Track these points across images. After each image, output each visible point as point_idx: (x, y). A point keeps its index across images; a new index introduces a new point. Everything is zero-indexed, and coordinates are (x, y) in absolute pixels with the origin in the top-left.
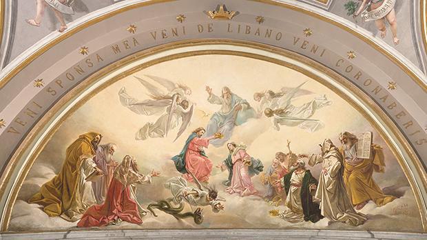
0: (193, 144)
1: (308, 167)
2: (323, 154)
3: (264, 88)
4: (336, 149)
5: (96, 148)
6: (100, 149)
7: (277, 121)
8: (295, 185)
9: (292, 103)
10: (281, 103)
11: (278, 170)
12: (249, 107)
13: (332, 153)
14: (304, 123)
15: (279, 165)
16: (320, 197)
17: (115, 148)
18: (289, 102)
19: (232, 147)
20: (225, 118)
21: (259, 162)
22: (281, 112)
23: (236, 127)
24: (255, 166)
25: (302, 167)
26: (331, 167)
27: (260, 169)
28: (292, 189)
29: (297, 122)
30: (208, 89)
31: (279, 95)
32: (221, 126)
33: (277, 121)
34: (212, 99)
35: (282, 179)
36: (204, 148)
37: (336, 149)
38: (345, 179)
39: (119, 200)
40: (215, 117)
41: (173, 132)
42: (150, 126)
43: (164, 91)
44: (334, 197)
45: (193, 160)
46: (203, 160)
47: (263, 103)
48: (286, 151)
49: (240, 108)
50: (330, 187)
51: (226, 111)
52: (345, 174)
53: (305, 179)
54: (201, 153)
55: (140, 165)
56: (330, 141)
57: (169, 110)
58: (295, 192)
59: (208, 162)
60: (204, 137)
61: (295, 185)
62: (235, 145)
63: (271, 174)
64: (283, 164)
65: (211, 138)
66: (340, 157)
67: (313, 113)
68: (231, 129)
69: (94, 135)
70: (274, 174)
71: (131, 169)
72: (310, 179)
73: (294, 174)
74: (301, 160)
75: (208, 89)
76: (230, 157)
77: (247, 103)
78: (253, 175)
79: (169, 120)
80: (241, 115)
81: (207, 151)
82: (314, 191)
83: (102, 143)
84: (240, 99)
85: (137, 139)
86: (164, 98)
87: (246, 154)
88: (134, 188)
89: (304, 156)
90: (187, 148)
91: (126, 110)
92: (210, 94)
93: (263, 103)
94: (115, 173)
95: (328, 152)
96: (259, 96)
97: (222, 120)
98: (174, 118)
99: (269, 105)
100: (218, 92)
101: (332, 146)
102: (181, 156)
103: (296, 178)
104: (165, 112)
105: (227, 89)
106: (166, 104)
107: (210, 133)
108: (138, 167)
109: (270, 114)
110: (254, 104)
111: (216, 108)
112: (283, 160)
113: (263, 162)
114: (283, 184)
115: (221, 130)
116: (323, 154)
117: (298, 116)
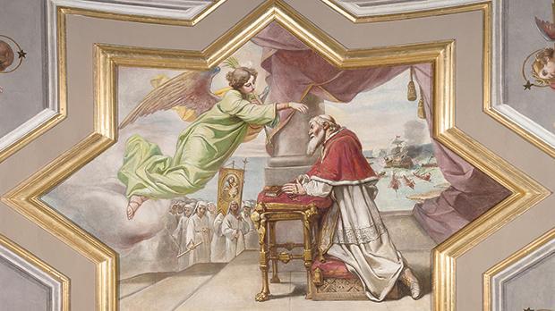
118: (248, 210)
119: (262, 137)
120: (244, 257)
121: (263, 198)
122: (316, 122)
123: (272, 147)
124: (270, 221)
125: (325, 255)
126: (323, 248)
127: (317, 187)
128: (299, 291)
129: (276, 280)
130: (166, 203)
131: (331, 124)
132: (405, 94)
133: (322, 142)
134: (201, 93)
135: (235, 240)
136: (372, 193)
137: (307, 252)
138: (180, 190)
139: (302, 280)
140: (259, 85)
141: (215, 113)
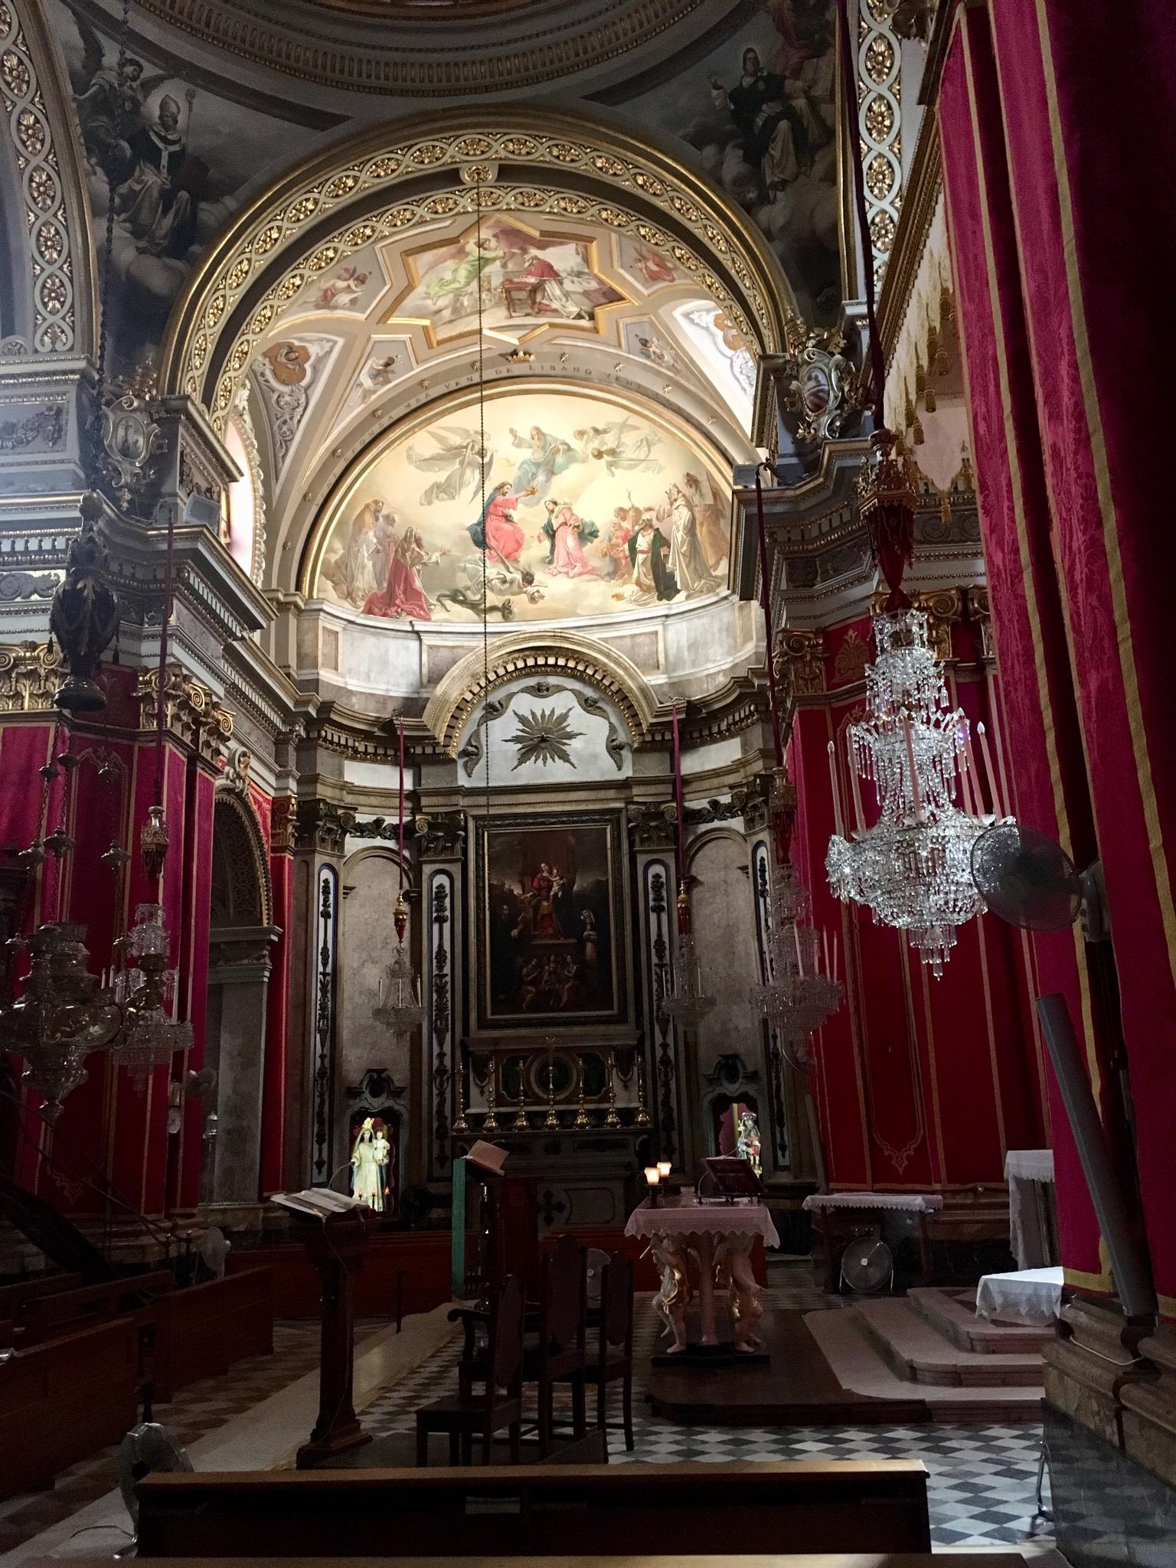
0: (496, 506)
1: (656, 524)
2: (671, 504)
3: (586, 425)
4: (684, 496)
5: (377, 519)
6: (381, 519)
7: (610, 465)
8: (643, 552)
9: (623, 440)
10: (610, 441)
11: (620, 533)
12: (569, 449)
13: (681, 501)
14: (643, 465)
15: (621, 528)
16: (674, 564)
17: (396, 518)
18: (619, 438)
19: (551, 506)
20: (538, 465)
21: (593, 524)
22: (612, 452)
23: (555, 478)
24: (587, 531)
25: (648, 525)
26: (682, 521)
27: (594, 534)
28: (640, 558)
29: (634, 463)
30: (512, 431)
31: (605, 432)
32: (534, 476)
33: (610, 465)
34: (518, 443)
35: (626, 546)
37: (684, 496)
39: (402, 587)
40: (525, 466)
42: (437, 486)
43: (456, 440)
45: (497, 529)
46: (511, 528)
47: (587, 442)
48: (627, 506)
49: (558, 451)
50: (685, 548)
51: (539, 456)
52: (698, 527)
53: (654, 541)
54: (507, 518)
55: (426, 539)
56: (675, 486)
57: (462, 463)
59: (520, 531)
60: (511, 495)
61: (643, 552)
62: (555, 503)
63: (610, 539)
65: (520, 494)
66: (690, 506)
67: (649, 451)
68: (548, 480)
69: (376, 502)
70: (614, 541)
71: (414, 545)
72: (660, 540)
73: (640, 536)
74: (646, 516)
75: (512, 431)
76: (549, 521)
77: (566, 444)
78: (585, 545)
79: (462, 475)
80: (560, 459)
81: (515, 515)
82: (666, 556)
83: (384, 512)
84: (556, 440)
85: (422, 504)
86: (456, 448)
87: (573, 514)
88: (419, 571)
89: (650, 509)
91: (412, 468)
92: (515, 436)
93: (587, 442)
94: (396, 551)
95: (676, 500)
96: (581, 434)
97: (534, 469)
98: (468, 472)
99: (596, 444)
100: (525, 433)
101: (679, 492)
102: (478, 524)
103: (643, 542)
104: (457, 466)
105: (537, 429)
106: (456, 456)
107: (519, 486)
108: (424, 543)
109: (599, 455)
110: (576, 444)
111: (526, 454)
112: (624, 519)
113: (599, 525)
114: (627, 553)
115: (534, 484)
116: (671, 504)
117: (634, 456)
118: (495, 289)
119: (498, 263)
120: (497, 305)
121: (503, 284)
122: (527, 257)
123: (504, 266)
124: (508, 291)
125: (540, 303)
126: (538, 300)
127: (532, 280)
128: (527, 315)
129: (515, 311)
130: (451, 295)
131: (536, 258)
132: (574, 252)
133: (531, 264)
134: (462, 253)
135: (490, 300)
136: (561, 283)
137: (530, 302)
138: (457, 289)
139: (529, 311)
140: (493, 243)
141: (470, 258)
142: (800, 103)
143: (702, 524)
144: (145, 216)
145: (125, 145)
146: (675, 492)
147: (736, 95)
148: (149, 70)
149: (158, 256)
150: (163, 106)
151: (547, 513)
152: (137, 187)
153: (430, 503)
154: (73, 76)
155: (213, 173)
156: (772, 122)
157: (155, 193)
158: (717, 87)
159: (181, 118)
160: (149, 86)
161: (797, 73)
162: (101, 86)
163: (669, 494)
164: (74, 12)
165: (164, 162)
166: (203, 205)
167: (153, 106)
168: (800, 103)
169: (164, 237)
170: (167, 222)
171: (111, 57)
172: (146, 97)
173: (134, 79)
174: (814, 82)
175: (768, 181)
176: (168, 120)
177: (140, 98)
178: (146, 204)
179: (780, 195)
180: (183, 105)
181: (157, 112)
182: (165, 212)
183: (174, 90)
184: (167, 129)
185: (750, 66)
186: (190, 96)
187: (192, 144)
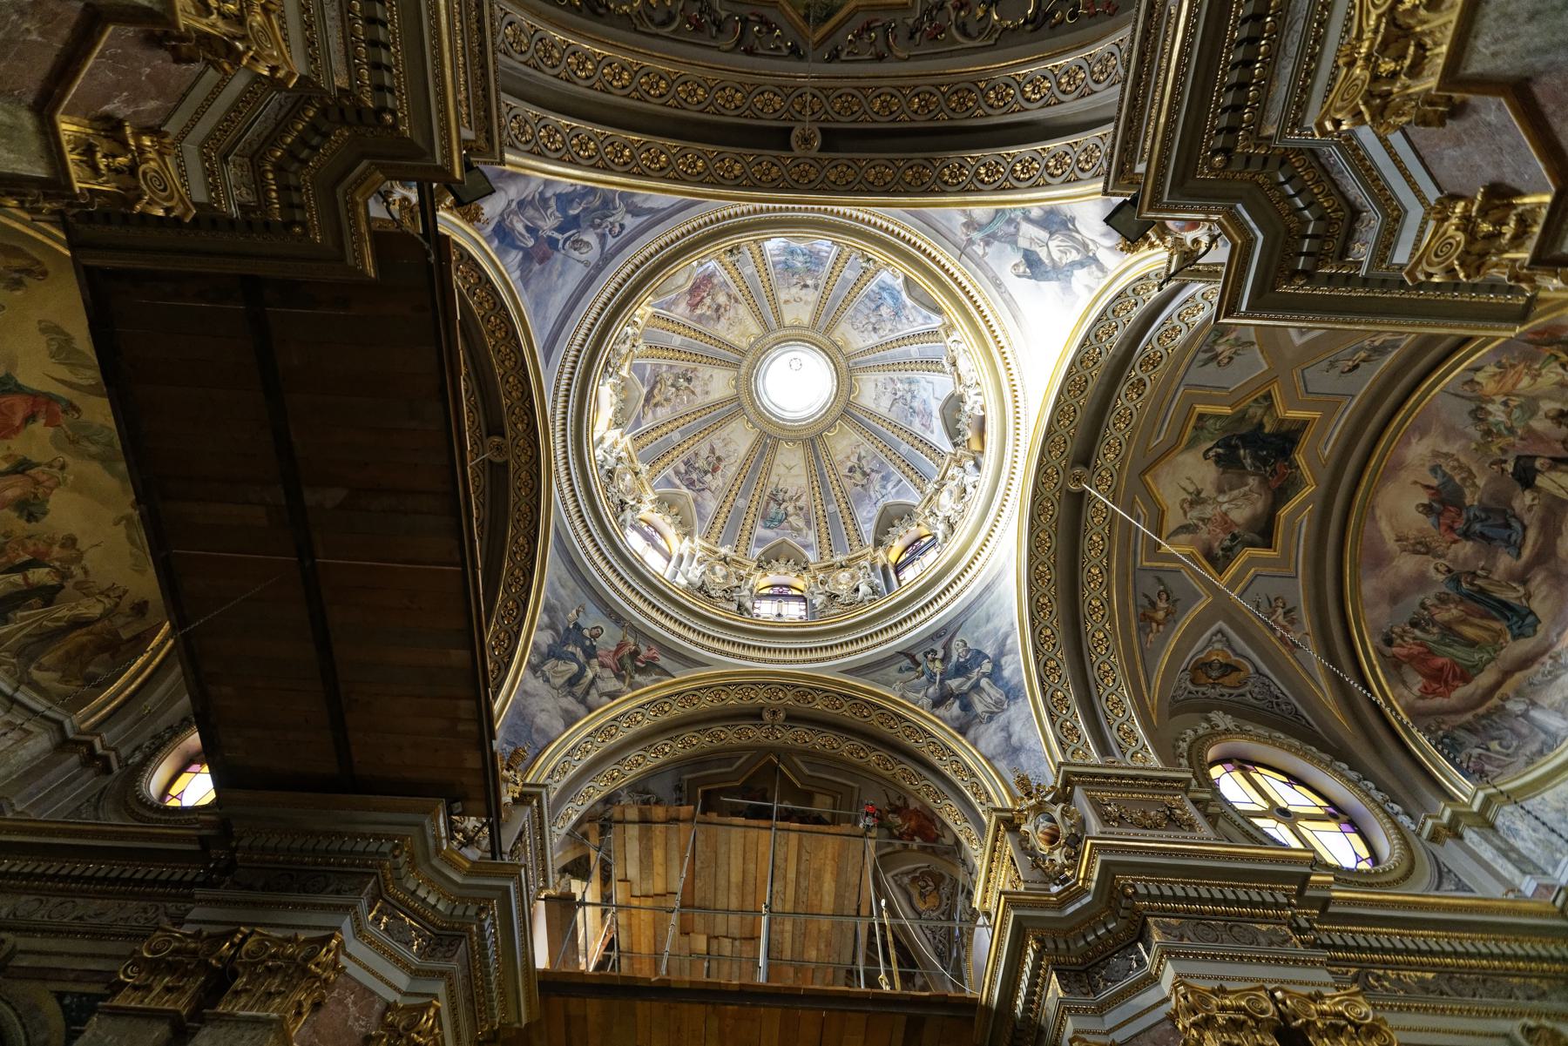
1: (69, 584)
2: (101, 593)
8: (26, 578)
11: (42, 547)
13: (108, 603)
16: (23, 619)
19: (56, 464)
21: (45, 513)
24: (33, 509)
25: (64, 575)
27: (31, 517)
28: (17, 578)
35: (27, 557)
36: (43, 421)
37: (117, 605)
38: (74, 634)
41: (64, 373)
42: (68, 340)
44: (35, 636)
46: (17, 423)
48: (83, 544)
50: (49, 624)
52: (84, 630)
54: (30, 418)
56: (125, 592)
58: (14, 584)
59: (17, 430)
60: (64, 420)
61: (26, 578)
63: (29, 537)
64: (56, 548)
66: (107, 614)
68: (93, 457)
70: (29, 543)
72: (48, 595)
73: (47, 570)
74: (76, 570)
76: (38, 465)
78: (15, 510)
82: (30, 607)
85: (40, 322)
87: (52, 489)
90: (35, 395)
95: (108, 596)
101: (120, 597)
103: (39, 575)
112: (63, 546)
113: (47, 519)
114: (18, 561)
142: (590, 674)
143: (90, 633)
144: (530, 212)
145: (576, 212)
146: (118, 593)
147: (578, 627)
148: (611, 241)
149: (502, 215)
150: (588, 244)
151: (47, 460)
152: (549, 212)
153: (43, 331)
154: (633, 195)
155: (536, 267)
156: (573, 658)
157: (540, 223)
158: (578, 612)
159: (576, 254)
160: (602, 238)
161: (603, 665)
162: (615, 208)
163: (112, 588)
164: (664, 209)
165: (556, 235)
166: (521, 255)
167: (591, 237)
168: (590, 674)
169: (511, 222)
170: (520, 227)
171: (630, 222)
172: (597, 234)
173: (610, 231)
174: (603, 679)
175: (545, 668)
176: (578, 244)
177: (599, 231)
178: (537, 215)
179: (541, 680)
180: (583, 257)
181: (585, 238)
182: (527, 228)
183: (593, 254)
184: (573, 242)
185: (594, 632)
186: (586, 264)
187: (559, 256)
